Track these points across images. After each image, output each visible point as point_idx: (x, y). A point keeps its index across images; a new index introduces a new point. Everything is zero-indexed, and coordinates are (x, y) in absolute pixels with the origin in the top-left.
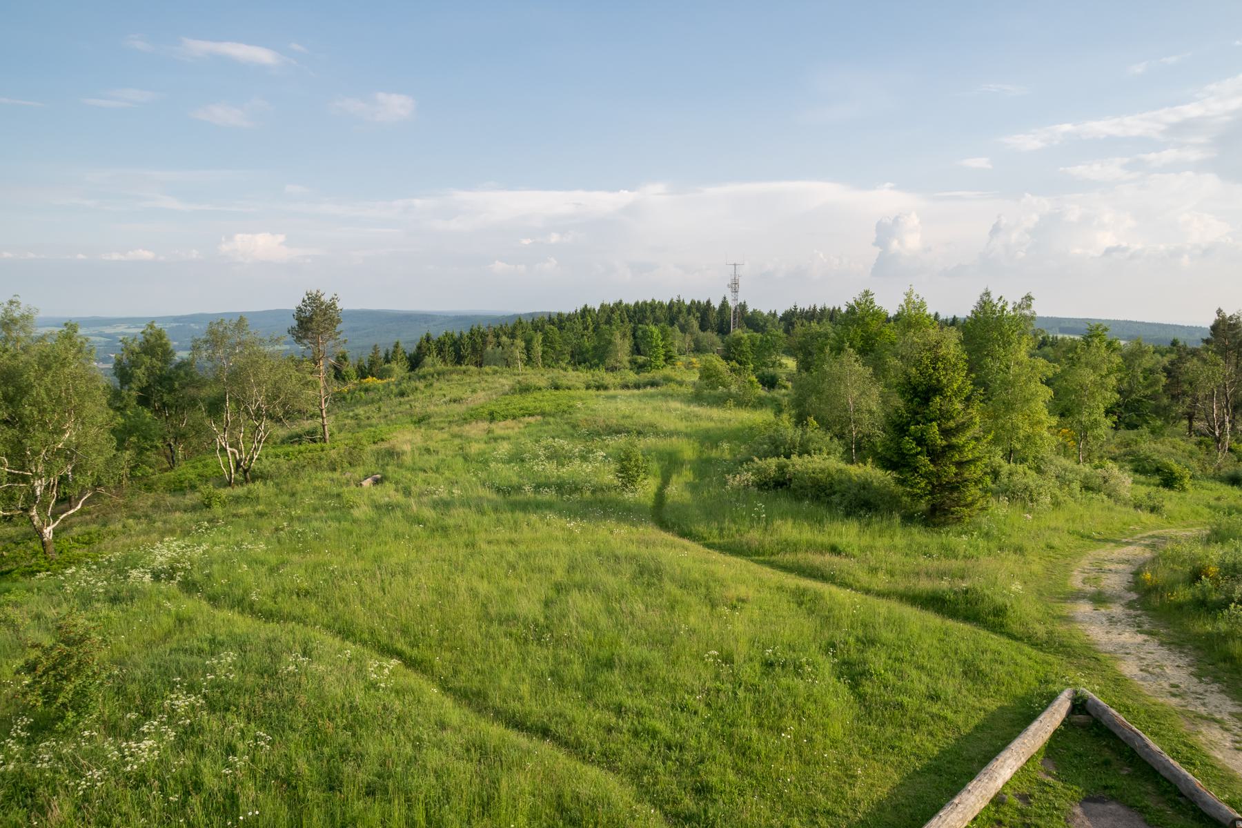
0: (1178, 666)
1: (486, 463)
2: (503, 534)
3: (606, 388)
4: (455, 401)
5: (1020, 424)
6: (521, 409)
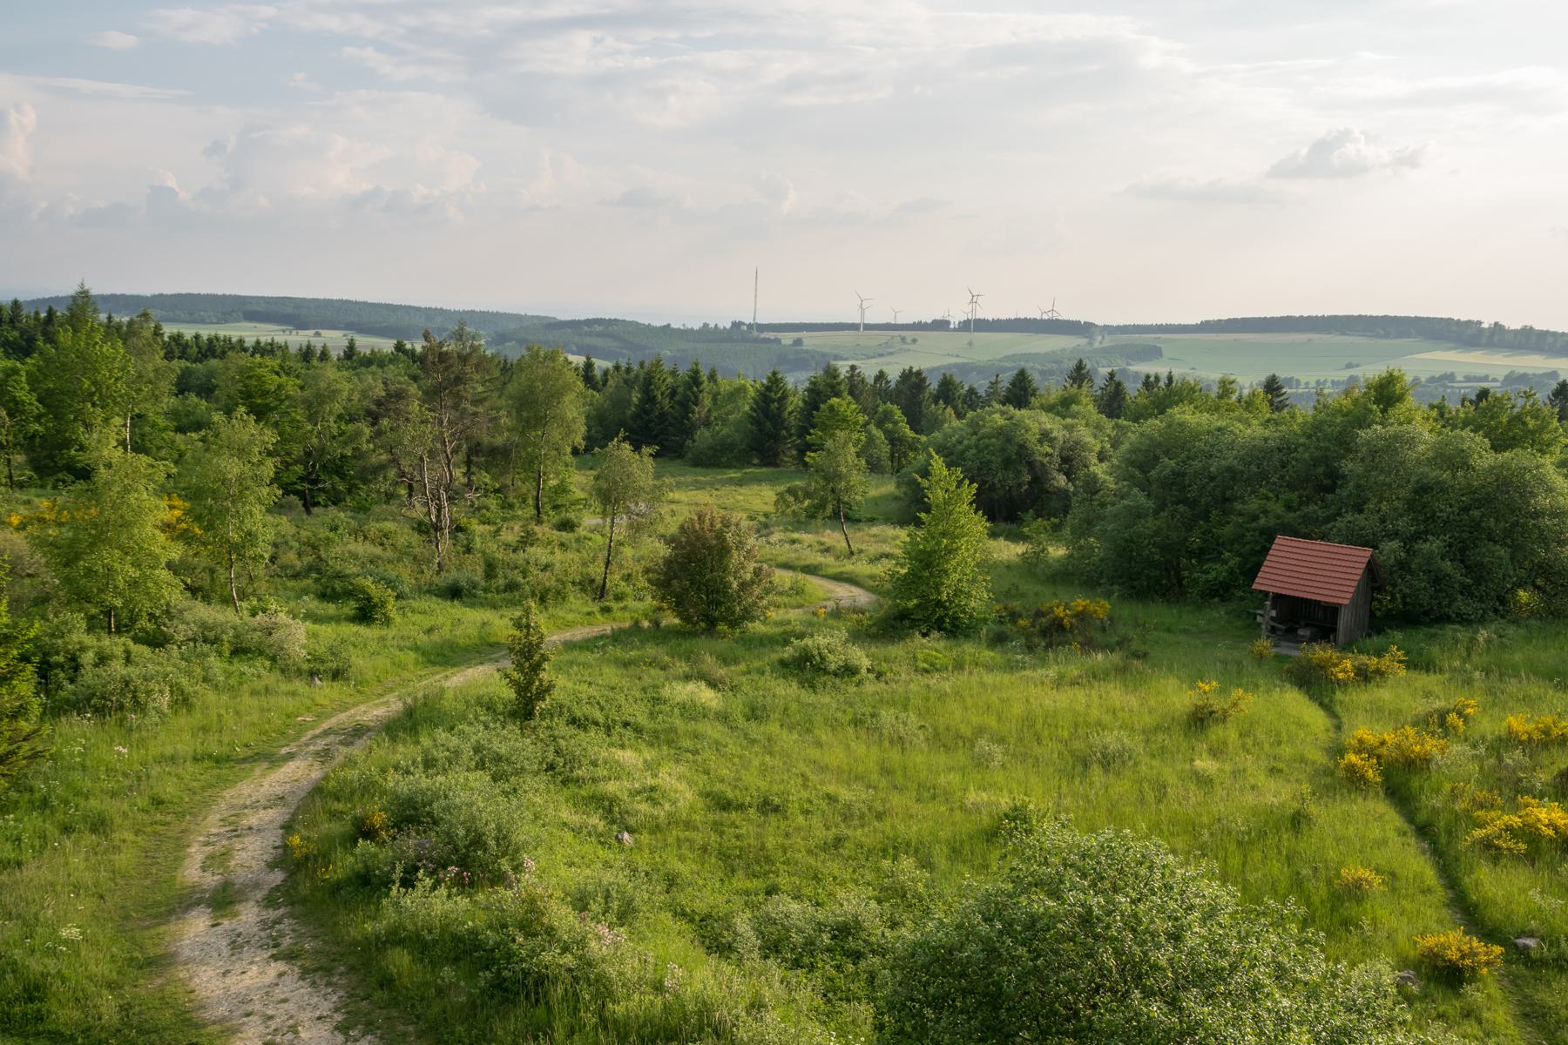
0: (319, 1018)
5: (117, 566)
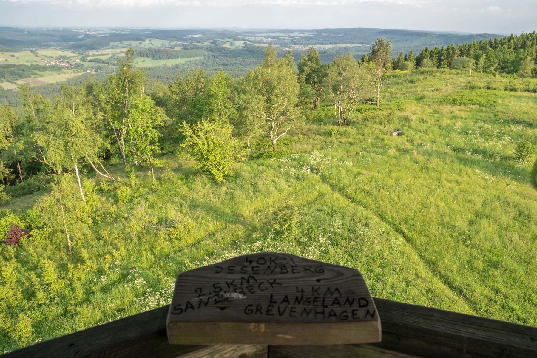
1: (449, 132)
2: (454, 176)
3: (516, 90)
4: (437, 90)
6: (469, 100)
